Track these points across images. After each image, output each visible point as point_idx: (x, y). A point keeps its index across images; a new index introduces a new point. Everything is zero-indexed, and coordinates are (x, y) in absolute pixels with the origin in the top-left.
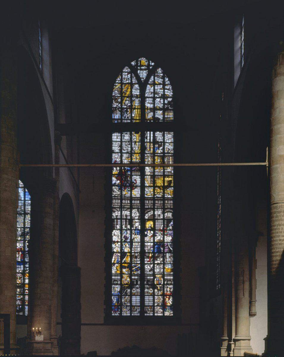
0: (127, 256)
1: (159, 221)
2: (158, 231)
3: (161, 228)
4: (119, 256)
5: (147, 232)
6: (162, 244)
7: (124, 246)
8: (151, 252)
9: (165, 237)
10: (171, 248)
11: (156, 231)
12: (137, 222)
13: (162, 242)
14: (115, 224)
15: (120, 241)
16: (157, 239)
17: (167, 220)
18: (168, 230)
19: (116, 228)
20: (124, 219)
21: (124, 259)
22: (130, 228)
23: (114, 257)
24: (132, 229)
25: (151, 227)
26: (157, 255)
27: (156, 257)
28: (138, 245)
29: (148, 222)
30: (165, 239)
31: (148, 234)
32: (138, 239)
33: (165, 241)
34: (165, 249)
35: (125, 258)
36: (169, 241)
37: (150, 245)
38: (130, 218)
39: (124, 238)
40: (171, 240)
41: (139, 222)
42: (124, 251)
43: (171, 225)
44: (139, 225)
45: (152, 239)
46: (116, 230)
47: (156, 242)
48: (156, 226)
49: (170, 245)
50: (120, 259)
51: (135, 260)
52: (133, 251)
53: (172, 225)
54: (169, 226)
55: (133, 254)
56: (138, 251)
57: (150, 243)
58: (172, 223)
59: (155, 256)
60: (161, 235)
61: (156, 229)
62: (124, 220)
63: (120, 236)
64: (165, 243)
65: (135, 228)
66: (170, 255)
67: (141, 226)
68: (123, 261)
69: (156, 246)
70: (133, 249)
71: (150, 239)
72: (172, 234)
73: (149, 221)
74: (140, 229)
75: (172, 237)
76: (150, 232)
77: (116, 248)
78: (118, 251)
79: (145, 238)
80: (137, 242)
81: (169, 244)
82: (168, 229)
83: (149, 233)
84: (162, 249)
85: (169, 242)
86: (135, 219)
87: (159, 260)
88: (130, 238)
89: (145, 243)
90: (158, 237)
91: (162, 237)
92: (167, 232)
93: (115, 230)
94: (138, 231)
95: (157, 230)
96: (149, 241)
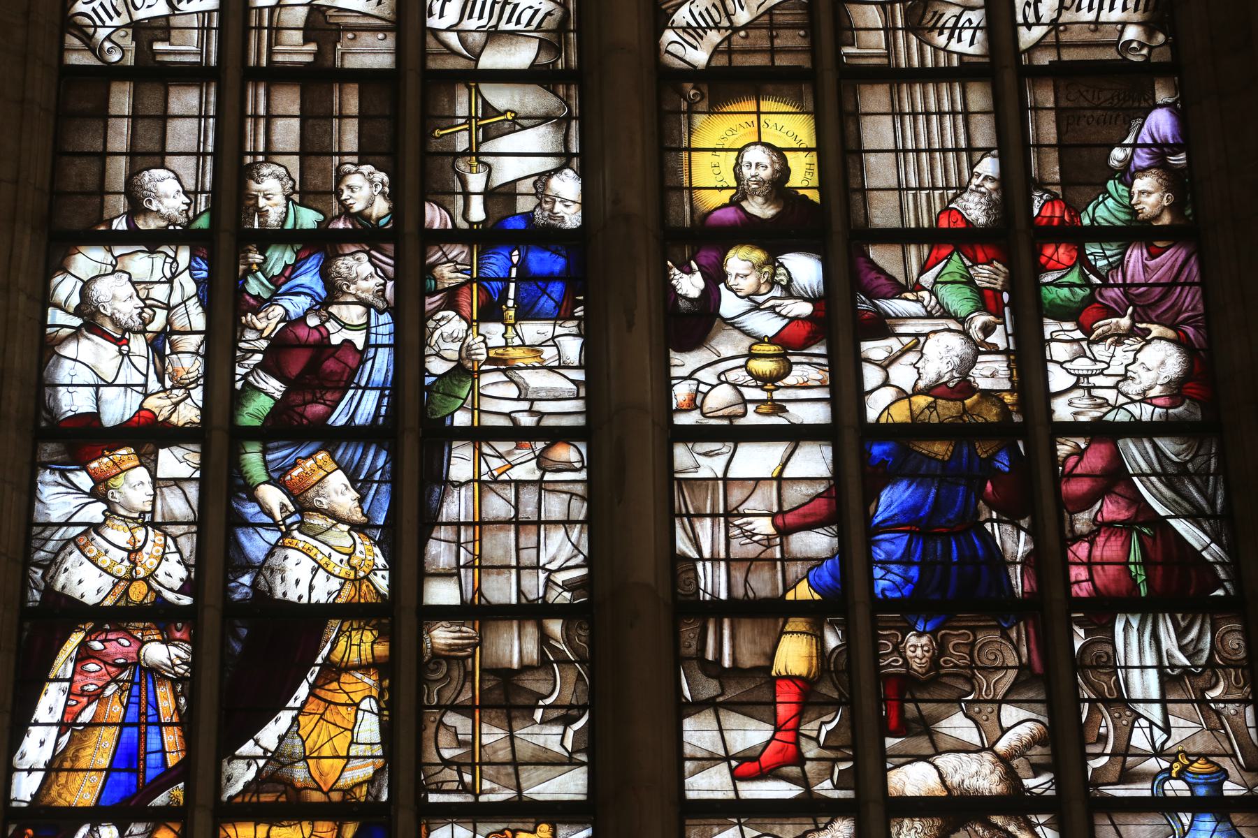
0: (333, 671)
1: (918, 97)
2: (914, 255)
3: (974, 209)
4: (153, 673)
5: (715, 276)
6: (1003, 463)
7: (273, 497)
8: (803, 592)
9: (1059, 351)
10: (1195, 517)
11: (883, 256)
12: (517, 123)
13: (1003, 431)
14: (119, 138)
15: (188, 414)
16: (903, 375)
17: (1060, 73)
18: (1101, 234)
19: (137, 207)
20: (277, 75)
21: (269, 735)
22: (381, 207)
23: (51, 703)
24: (434, 216)
25: (778, 187)
26: (917, 647)
27: (908, 684)
28: (540, 483)
29: (713, 109)
30: (1058, 379)
31: (730, 305)
32: (537, 380)
33: (1062, 411)
34: (1082, 550)
35: (285, 717)
36: (1146, 413)
37: (779, 479)
38: (384, 61)
39: (270, 365)
40: (1177, 390)
41: (561, 123)
42: (263, 599)
43: (1142, 158)
44: (565, 158)
45: (807, 372)
46: (133, 237)
47: (884, 431)
48: (880, 170)
49: (1172, 476)
50: (172, 738)
51: (492, 735)
52: (442, 593)
53: (1160, 150)
54: (1111, 173)
55: (442, 636)
56: (534, 585)
57: (776, 451)
58: (1160, 123)
59: (892, 664)
60: (980, 319)
61: (883, 214)
62: (289, 100)
63: (192, 342)
64: (1063, 449)
65: (477, 212)
66: (1191, 651)
67: (583, 175)
68: (241, 775)
69: (892, 499)
70: (439, 552)
71: (765, 381)
72: (1189, 299)
73: (737, 97)
74: (571, 217)
75: (1180, 342)
76: (773, 260)
77: (118, 534)
78: (138, 593)
79: (683, 363)
80: (516, 434)
81: (1135, 454)
82: (1105, 212)
83: (747, 285)
84: (1016, 544)
85: (1136, 429)
86: (477, 77)
87: (970, 734)
88: (381, 365)
89: (682, 455)
90: (917, 344)
91: (998, 338)
92: (1082, 260)
93: (109, 239)
94: (545, 261)
95: (900, 237)
96: (752, 419)
